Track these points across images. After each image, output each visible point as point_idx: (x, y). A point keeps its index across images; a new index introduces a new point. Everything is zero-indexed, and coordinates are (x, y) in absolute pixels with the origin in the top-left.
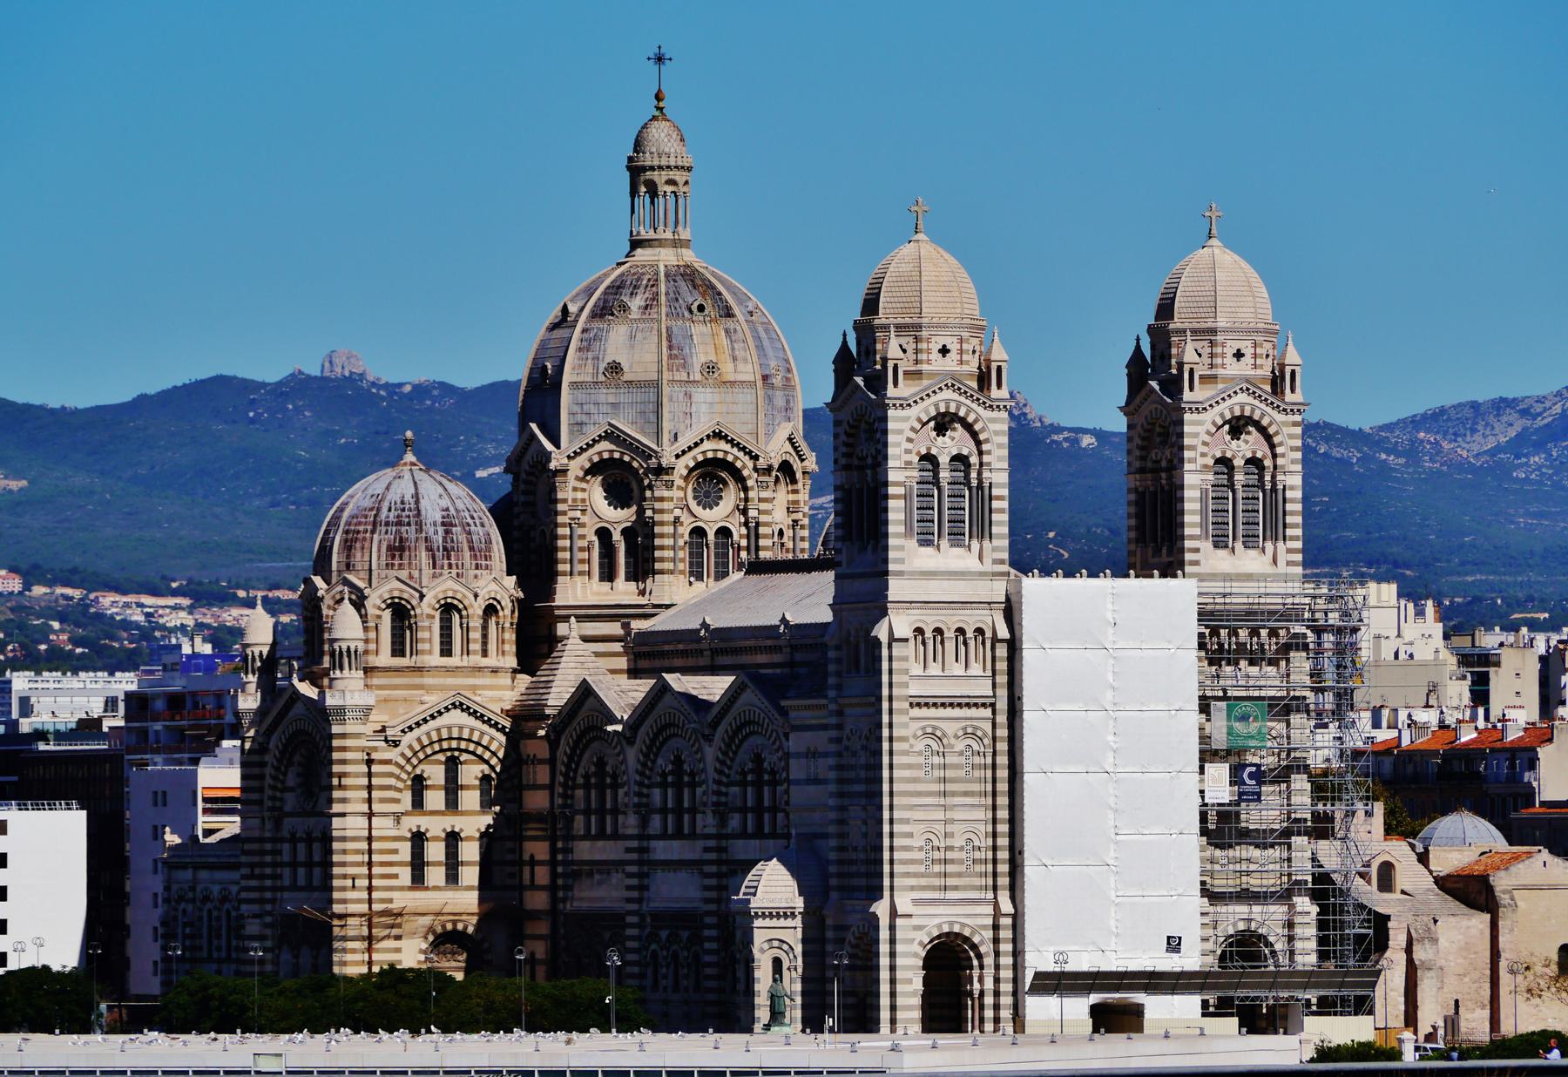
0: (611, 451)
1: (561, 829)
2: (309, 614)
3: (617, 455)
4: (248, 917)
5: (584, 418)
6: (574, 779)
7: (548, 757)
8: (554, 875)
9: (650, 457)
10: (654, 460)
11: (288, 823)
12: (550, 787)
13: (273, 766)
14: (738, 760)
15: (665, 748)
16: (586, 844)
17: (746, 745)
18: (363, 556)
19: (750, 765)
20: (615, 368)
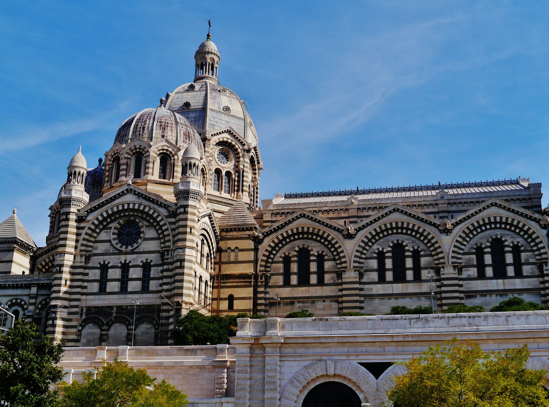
0: (228, 139)
1: (262, 282)
2: (129, 156)
3: (230, 141)
4: (60, 307)
5: (215, 124)
6: (272, 259)
7: (253, 247)
8: (255, 304)
9: (244, 145)
10: (246, 146)
11: (95, 261)
12: (256, 262)
13: (89, 228)
14: (473, 242)
15: (382, 240)
16: (288, 289)
17: (480, 235)
18: (172, 134)
19: (489, 244)
20: (227, 109)
